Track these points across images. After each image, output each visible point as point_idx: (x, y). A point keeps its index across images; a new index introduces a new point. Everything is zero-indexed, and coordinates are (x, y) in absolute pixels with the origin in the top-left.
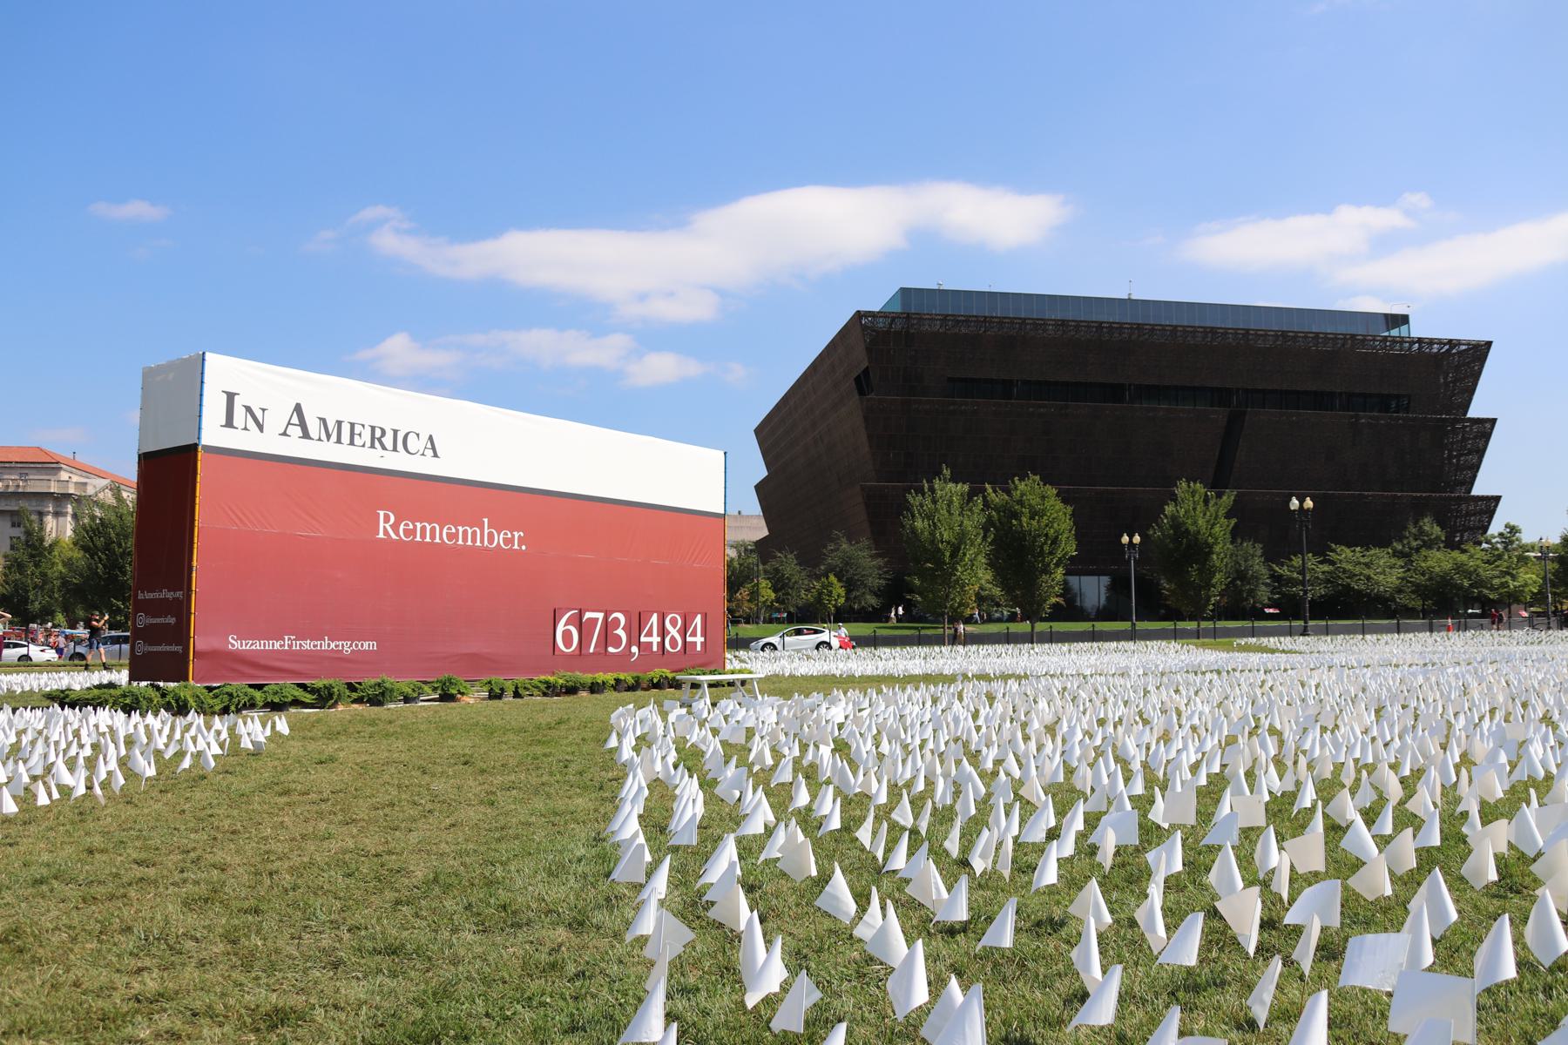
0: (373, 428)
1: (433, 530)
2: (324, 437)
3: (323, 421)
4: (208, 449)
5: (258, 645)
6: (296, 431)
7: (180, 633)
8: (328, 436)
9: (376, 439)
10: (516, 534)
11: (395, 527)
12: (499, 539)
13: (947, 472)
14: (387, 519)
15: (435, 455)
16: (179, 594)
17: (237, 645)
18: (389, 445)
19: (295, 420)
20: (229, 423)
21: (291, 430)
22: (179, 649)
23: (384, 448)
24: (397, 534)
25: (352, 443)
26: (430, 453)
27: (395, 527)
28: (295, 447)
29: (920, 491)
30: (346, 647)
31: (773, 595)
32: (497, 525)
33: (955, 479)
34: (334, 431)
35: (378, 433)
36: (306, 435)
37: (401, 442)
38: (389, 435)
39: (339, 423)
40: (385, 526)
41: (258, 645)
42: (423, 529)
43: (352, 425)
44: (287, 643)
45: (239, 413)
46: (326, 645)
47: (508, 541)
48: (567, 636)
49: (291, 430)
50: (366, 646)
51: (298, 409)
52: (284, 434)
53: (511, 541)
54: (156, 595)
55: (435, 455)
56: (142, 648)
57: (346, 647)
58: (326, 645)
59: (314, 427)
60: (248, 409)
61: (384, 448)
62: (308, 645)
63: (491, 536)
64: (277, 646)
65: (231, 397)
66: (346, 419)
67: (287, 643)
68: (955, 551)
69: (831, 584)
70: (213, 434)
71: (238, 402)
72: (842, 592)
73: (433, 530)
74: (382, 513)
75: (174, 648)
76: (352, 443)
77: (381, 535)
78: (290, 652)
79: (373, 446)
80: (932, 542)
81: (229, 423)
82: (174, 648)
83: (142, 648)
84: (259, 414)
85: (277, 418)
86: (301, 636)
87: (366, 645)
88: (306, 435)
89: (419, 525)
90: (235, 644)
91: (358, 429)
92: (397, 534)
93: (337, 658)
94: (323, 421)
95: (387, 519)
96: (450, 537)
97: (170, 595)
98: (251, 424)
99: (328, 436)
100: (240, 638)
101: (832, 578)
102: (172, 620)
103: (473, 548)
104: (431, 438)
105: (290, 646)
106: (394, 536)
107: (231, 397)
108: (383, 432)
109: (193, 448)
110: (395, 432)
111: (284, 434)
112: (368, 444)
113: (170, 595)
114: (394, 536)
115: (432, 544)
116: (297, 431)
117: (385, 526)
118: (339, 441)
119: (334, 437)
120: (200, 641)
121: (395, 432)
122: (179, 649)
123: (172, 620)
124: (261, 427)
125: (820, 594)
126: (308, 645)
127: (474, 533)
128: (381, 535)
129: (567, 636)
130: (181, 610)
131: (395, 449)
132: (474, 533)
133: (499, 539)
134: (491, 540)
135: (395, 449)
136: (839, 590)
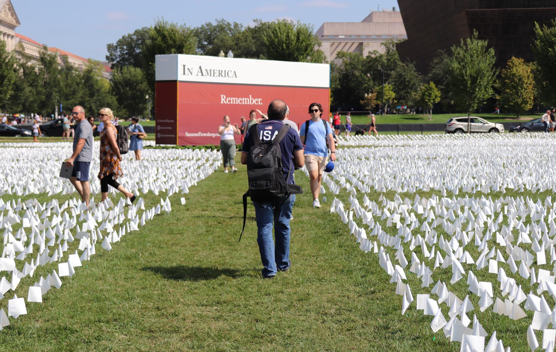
4: (180, 81)
7: (174, 131)
9: (220, 74)
11: (226, 100)
12: (254, 101)
13: (476, 34)
14: (223, 97)
16: (172, 121)
18: (223, 75)
19: (200, 71)
20: (184, 74)
22: (174, 136)
27: (226, 100)
29: (458, 45)
31: (393, 95)
33: (480, 38)
34: (210, 73)
36: (202, 75)
37: (227, 74)
40: (224, 100)
44: (200, 134)
45: (187, 71)
46: (209, 135)
47: (257, 102)
51: (200, 67)
54: (164, 121)
56: (159, 135)
58: (209, 135)
62: (204, 135)
63: (252, 101)
65: (184, 66)
66: (212, 69)
67: (200, 134)
68: (474, 80)
69: (431, 89)
70: (181, 77)
71: (186, 67)
72: (438, 93)
74: (222, 96)
75: (172, 136)
78: (200, 137)
80: (462, 75)
81: (184, 74)
82: (172, 136)
83: (159, 135)
85: (196, 70)
86: (203, 132)
88: (202, 75)
90: (187, 135)
91: (215, 71)
93: (211, 138)
95: (223, 97)
96: (241, 101)
97: (169, 121)
100: (189, 133)
101: (432, 84)
102: (171, 128)
107: (184, 66)
109: (175, 82)
113: (169, 121)
116: (200, 74)
120: (179, 134)
122: (174, 136)
123: (171, 128)
125: (424, 95)
126: (204, 135)
128: (222, 102)
130: (174, 125)
133: (254, 101)
134: (252, 101)
136: (436, 94)
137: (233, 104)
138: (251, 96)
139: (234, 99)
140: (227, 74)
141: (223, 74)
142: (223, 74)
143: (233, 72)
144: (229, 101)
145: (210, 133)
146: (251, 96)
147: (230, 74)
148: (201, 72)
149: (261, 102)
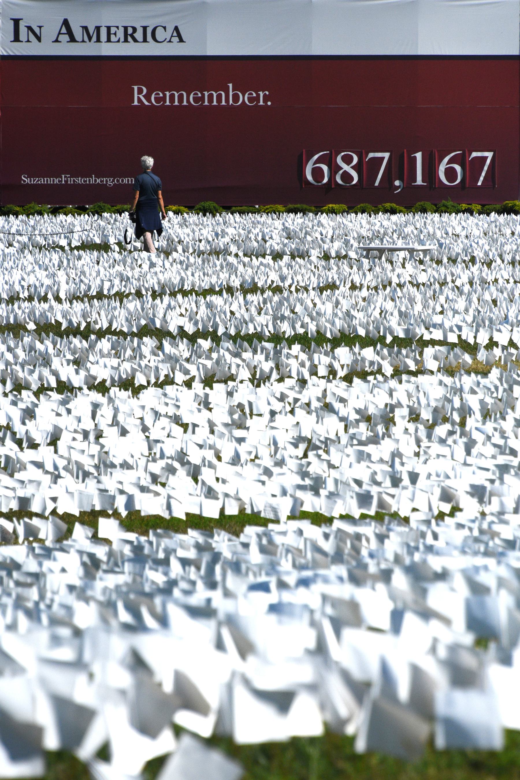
0: (126, 28)
1: (181, 97)
2: (86, 38)
3: (85, 28)
5: (43, 181)
6: (65, 38)
8: (90, 38)
9: (129, 35)
10: (261, 94)
12: (244, 98)
15: (181, 40)
17: (27, 181)
19: (64, 30)
21: (61, 38)
23: (135, 40)
24: (149, 100)
25: (109, 40)
26: (177, 39)
27: (148, 97)
28: (66, 49)
30: (110, 182)
34: (92, 34)
35: (130, 31)
36: (73, 39)
37: (150, 34)
38: (140, 31)
39: (98, 28)
40: (139, 96)
41: (43, 181)
42: (172, 97)
43: (109, 28)
46: (93, 180)
47: (250, 99)
48: (317, 173)
49: (61, 38)
50: (125, 181)
51: (66, 23)
52: (57, 41)
53: (258, 98)
55: (181, 40)
57: (110, 182)
58: (93, 180)
59: (78, 33)
60: (30, 28)
61: (135, 40)
62: (80, 181)
63: (236, 98)
64: (56, 181)
65: (16, 22)
66: (104, 23)
73: (181, 97)
74: (136, 88)
76: (109, 40)
77: (136, 103)
79: (126, 40)
81: (17, 39)
84: (37, 30)
87: (125, 181)
88: (73, 39)
89: (168, 94)
90: (26, 180)
91: (113, 30)
92: (149, 100)
94: (85, 28)
95: (140, 91)
98: (32, 37)
99: (90, 38)
100: (29, 176)
104: (176, 29)
105: (66, 181)
106: (146, 103)
107: (16, 22)
108: (135, 30)
110: (145, 28)
111: (57, 41)
112: (122, 39)
114: (146, 103)
115: (181, 106)
116: (67, 38)
117: (139, 96)
118: (98, 40)
119: (94, 38)
121: (145, 28)
124: (39, 39)
126: (80, 181)
127: (219, 97)
128: (136, 103)
129: (317, 173)
131: (145, 40)
132: (219, 97)
133: (244, 98)
134: (236, 98)
135: (145, 40)
137: (172, 107)
138: (231, 85)
139: (176, 95)
140: (150, 34)
141: (139, 35)
142: (139, 35)
143: (170, 29)
144: (157, 100)
145: (97, 176)
146: (231, 85)
147: (160, 34)
148: (70, 32)
149: (266, 98)
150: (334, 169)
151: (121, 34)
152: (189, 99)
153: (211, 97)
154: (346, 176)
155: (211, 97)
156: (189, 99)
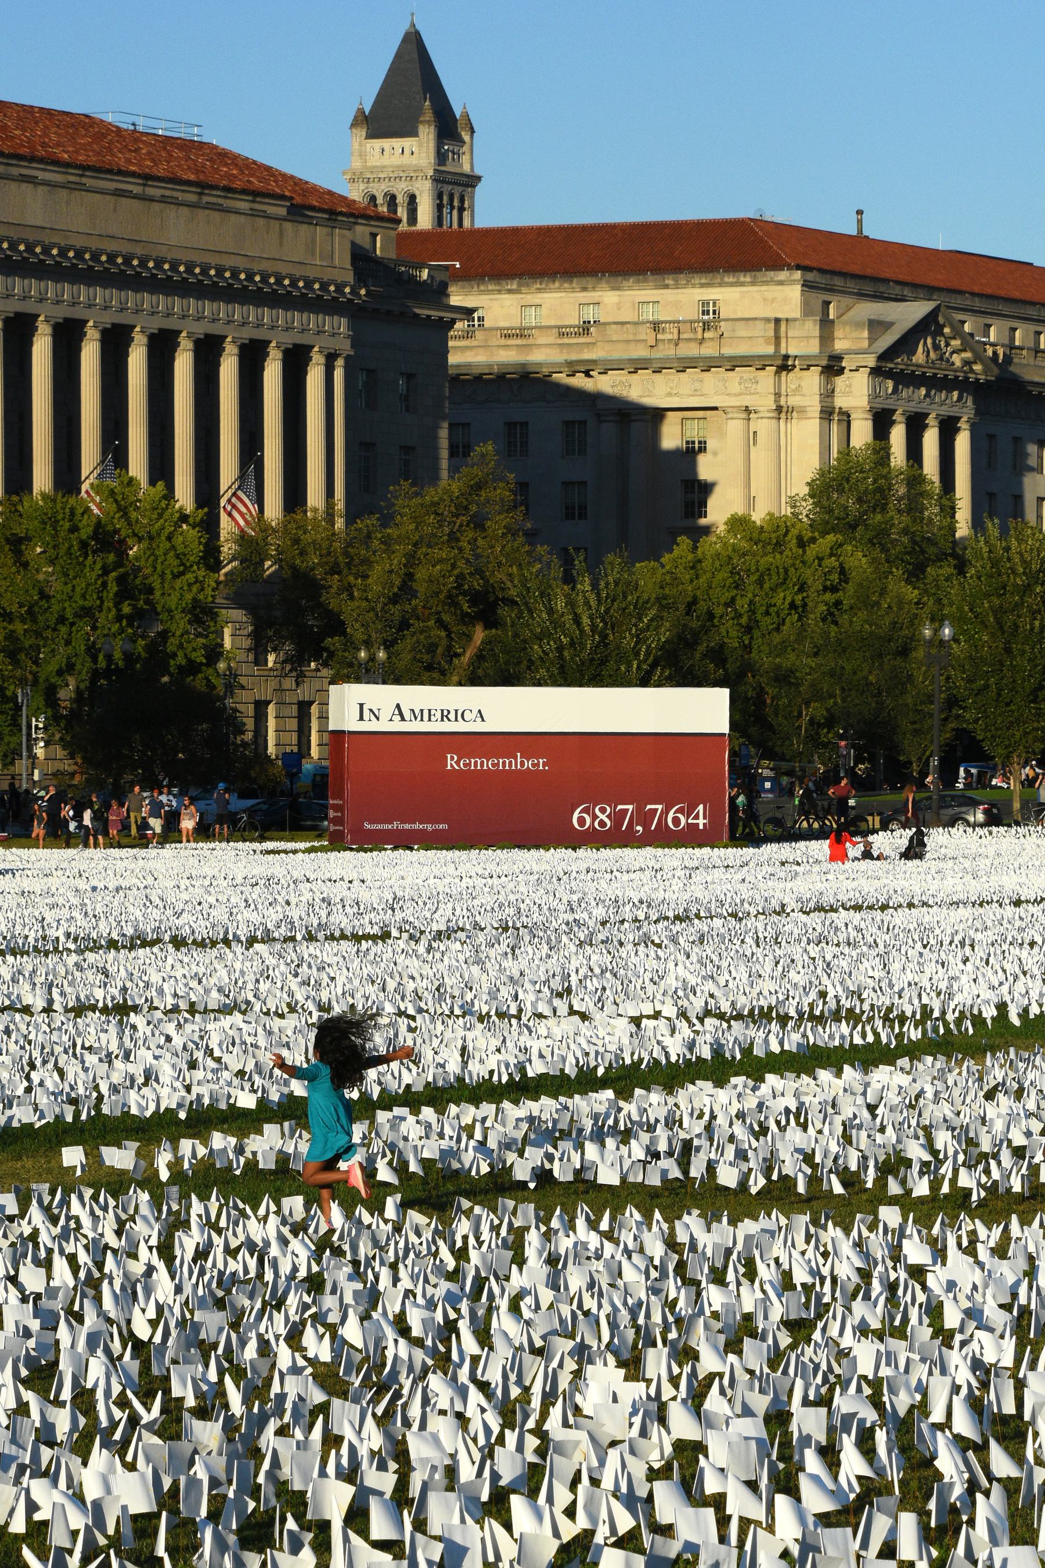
1: (482, 763)
3: (413, 711)
9: (444, 716)
12: (528, 764)
14: (452, 758)
20: (361, 718)
27: (458, 763)
28: (398, 726)
32: (527, 756)
36: (403, 719)
40: (451, 762)
45: (366, 713)
48: (582, 821)
51: (398, 706)
53: (538, 764)
59: (407, 715)
65: (361, 705)
71: (365, 707)
73: (482, 763)
81: (361, 718)
88: (403, 719)
95: (452, 758)
103: (510, 771)
107: (361, 705)
117: (451, 762)
129: (582, 821)
133: (528, 764)
137: (476, 770)
141: (452, 716)
142: (452, 716)
143: (475, 712)
144: (465, 765)
148: (401, 714)
150: (595, 817)
151: (439, 715)
152: (488, 764)
153: (504, 763)
154: (602, 824)
155: (504, 763)
156: (488, 764)
